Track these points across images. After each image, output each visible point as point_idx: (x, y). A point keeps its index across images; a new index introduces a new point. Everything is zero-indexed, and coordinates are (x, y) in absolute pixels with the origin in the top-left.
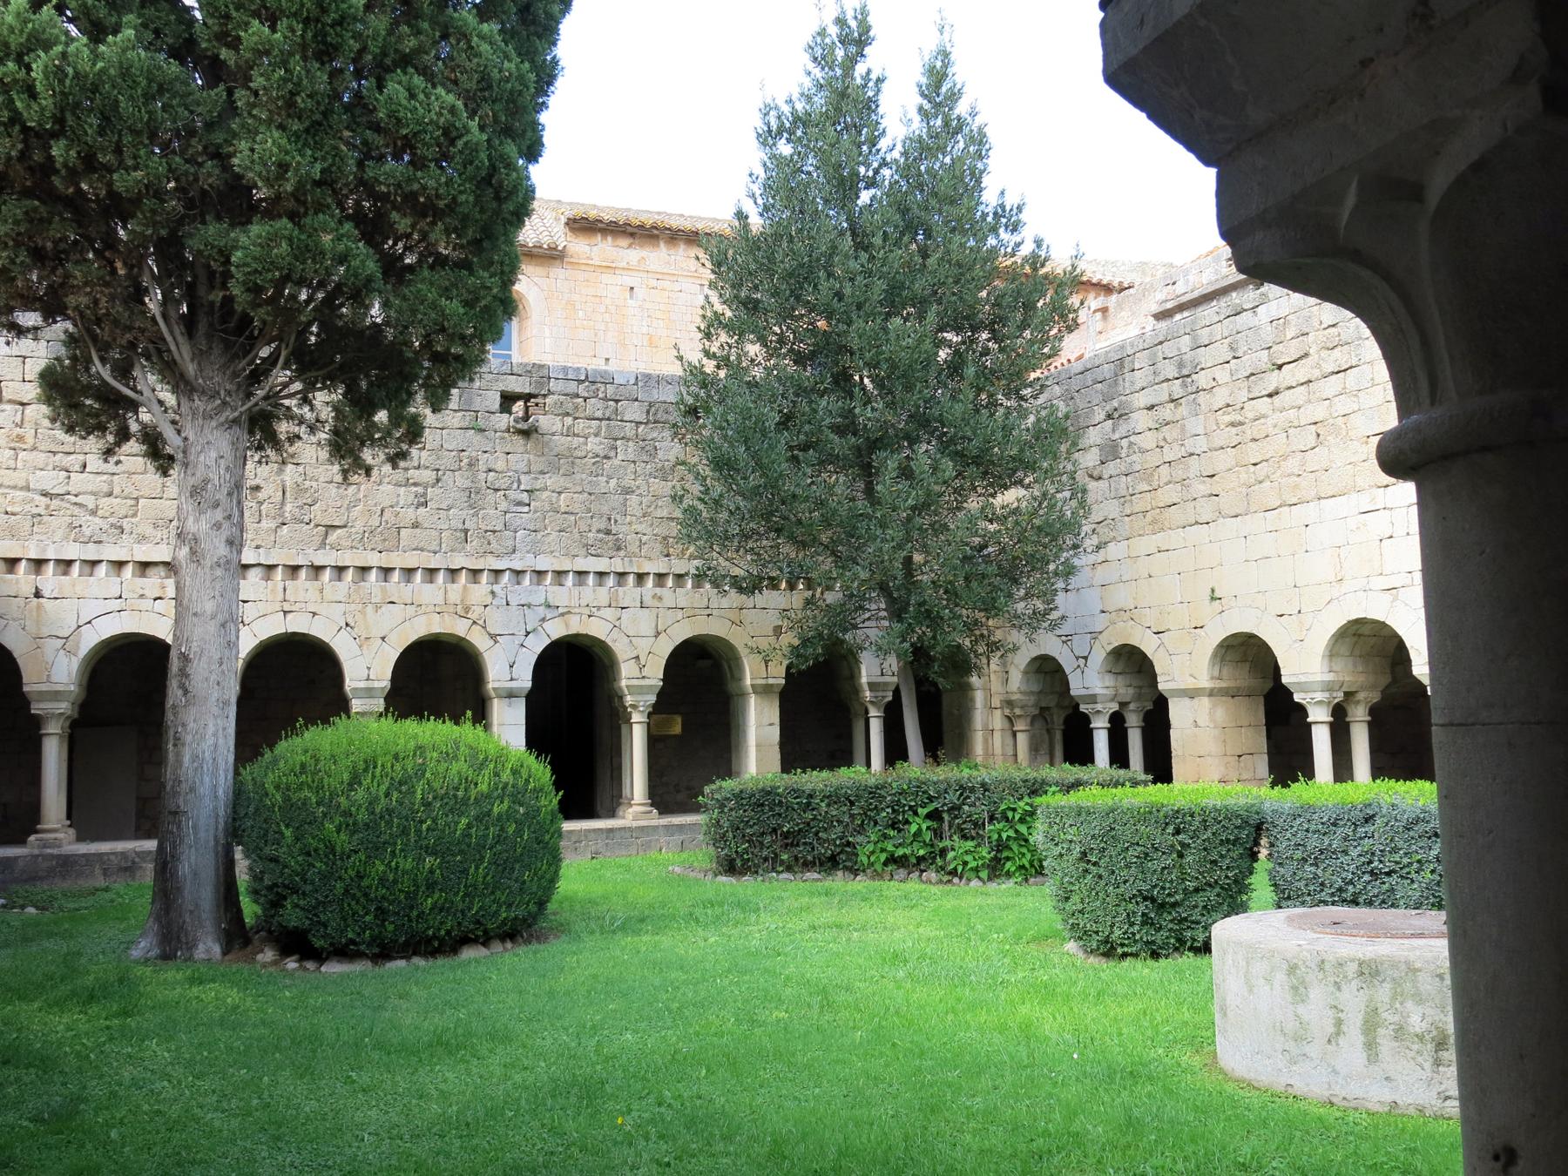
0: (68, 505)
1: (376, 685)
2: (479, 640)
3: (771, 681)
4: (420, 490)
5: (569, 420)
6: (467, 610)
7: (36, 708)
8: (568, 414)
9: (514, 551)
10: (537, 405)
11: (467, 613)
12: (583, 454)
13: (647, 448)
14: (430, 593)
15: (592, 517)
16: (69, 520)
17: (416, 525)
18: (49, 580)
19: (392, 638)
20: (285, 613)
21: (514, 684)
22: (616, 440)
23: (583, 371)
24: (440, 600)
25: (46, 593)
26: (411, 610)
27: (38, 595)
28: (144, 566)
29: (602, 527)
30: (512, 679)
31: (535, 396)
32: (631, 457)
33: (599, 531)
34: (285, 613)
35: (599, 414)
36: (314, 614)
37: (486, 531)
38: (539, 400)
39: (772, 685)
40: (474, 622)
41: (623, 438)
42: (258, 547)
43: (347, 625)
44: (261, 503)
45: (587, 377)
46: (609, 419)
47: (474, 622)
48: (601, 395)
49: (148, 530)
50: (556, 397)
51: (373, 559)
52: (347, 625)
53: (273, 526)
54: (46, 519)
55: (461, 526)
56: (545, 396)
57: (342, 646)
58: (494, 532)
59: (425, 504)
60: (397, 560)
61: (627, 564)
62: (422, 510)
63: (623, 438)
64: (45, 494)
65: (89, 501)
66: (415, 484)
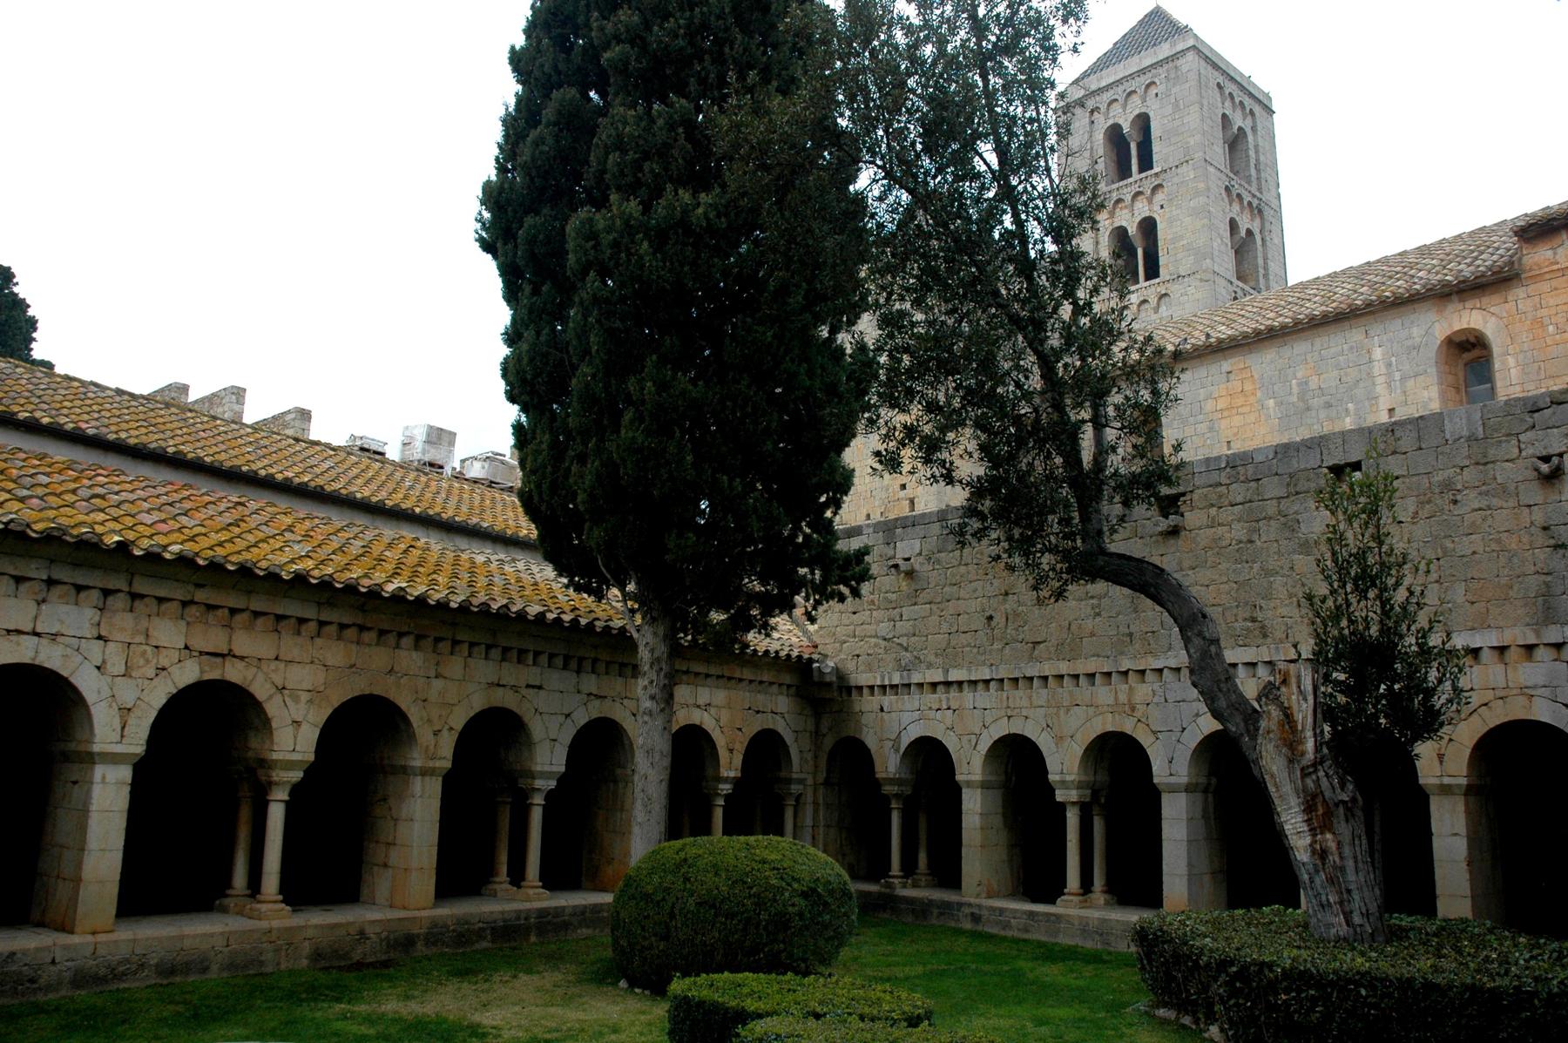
0: (894, 645)
1: (1068, 778)
2: (1144, 739)
3: (1446, 781)
4: (1095, 601)
5: (1213, 511)
6: (1133, 709)
7: (888, 789)
8: (1213, 505)
9: (1170, 649)
10: (1185, 502)
11: (1133, 711)
12: (1228, 542)
13: (1290, 523)
14: (1103, 693)
15: (1237, 607)
16: (894, 655)
17: (1092, 635)
18: (888, 700)
19: (1078, 736)
20: (1009, 717)
21: (1172, 780)
22: (1258, 521)
23: (1224, 458)
24: (1111, 701)
25: (885, 709)
26: (1091, 710)
27: (882, 710)
28: (934, 685)
29: (1247, 615)
30: (1171, 775)
31: (1183, 494)
32: (1272, 537)
33: (1245, 620)
34: (1009, 717)
35: (1239, 499)
36: (1027, 717)
37: (1147, 633)
38: (1188, 497)
39: (1450, 786)
40: (1139, 720)
41: (1265, 518)
42: (992, 665)
43: (1048, 726)
44: (993, 629)
45: (1228, 462)
46: (1250, 501)
47: (1139, 720)
48: (1242, 478)
49: (932, 658)
50: (1200, 491)
51: (1064, 668)
52: (1048, 726)
53: (1000, 647)
54: (884, 656)
55: (1127, 631)
56: (1191, 492)
57: (1044, 742)
58: (1153, 632)
59: (1098, 614)
60: (1081, 667)
61: (1273, 651)
62: (1098, 619)
63: (1265, 518)
64: (885, 639)
65: (903, 641)
66: (1092, 597)
